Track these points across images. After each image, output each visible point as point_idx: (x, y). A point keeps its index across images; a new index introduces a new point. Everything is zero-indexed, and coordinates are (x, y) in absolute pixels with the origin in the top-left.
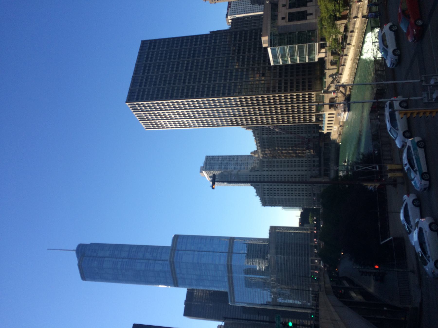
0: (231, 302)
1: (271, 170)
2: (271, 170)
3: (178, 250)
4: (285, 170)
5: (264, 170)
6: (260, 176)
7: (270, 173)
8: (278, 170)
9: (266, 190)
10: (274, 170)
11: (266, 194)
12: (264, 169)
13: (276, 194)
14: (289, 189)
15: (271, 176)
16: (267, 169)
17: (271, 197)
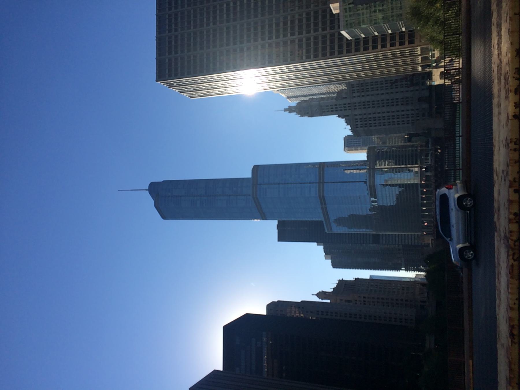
0: (328, 230)
1: (363, 96)
2: (363, 96)
3: (260, 184)
4: (383, 94)
5: (355, 97)
6: (349, 104)
7: (363, 99)
8: (372, 95)
9: (359, 120)
10: (368, 95)
11: (359, 126)
12: (354, 95)
13: (373, 125)
14: (389, 116)
15: (364, 102)
16: (358, 94)
17: (366, 128)
